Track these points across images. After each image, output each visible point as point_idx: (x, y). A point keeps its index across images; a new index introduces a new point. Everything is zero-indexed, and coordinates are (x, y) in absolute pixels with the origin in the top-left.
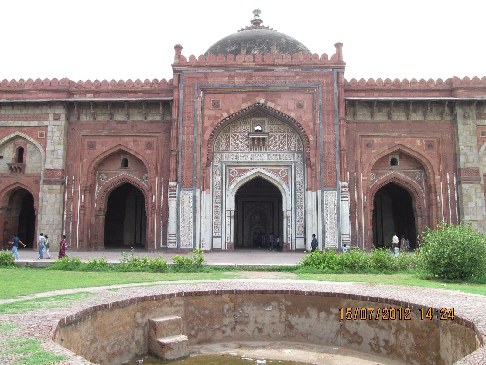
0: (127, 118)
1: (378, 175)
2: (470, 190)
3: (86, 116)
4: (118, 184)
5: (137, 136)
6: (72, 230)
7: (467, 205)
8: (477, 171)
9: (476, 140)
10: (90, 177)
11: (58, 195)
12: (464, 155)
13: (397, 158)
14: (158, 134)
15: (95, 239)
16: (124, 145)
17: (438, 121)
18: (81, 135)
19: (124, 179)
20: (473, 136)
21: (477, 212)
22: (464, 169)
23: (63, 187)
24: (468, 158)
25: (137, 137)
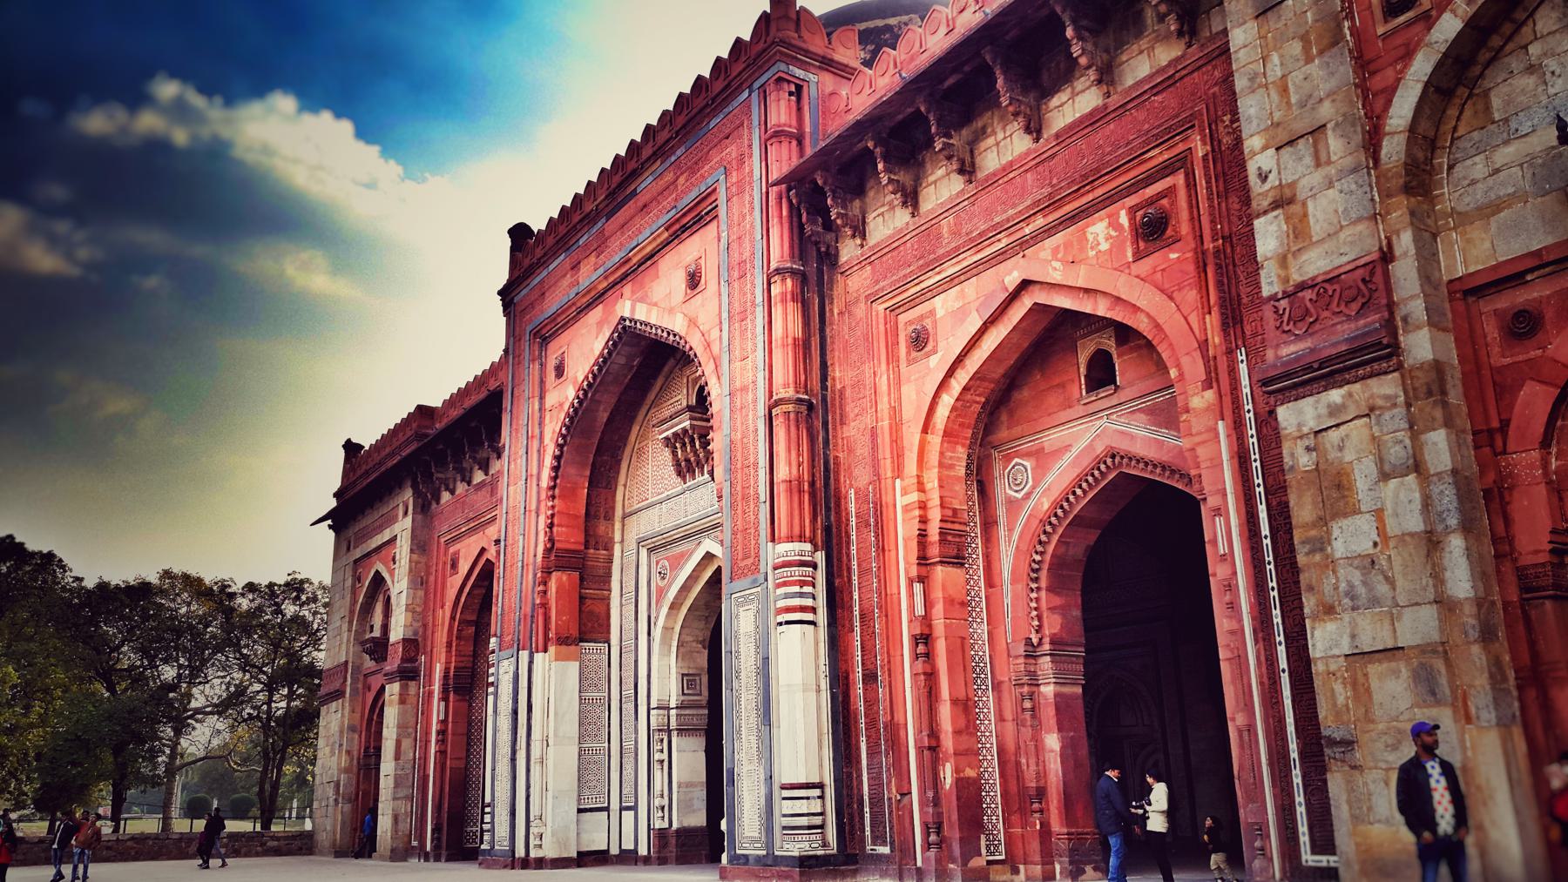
1: (1042, 458)
2: (1334, 436)
7: (1321, 545)
8: (1367, 284)
9: (1345, 70)
12: (1277, 204)
13: (1110, 345)
17: (1169, 65)
20: (1321, 52)
21: (1391, 582)
22: (1284, 303)
24: (1305, 215)
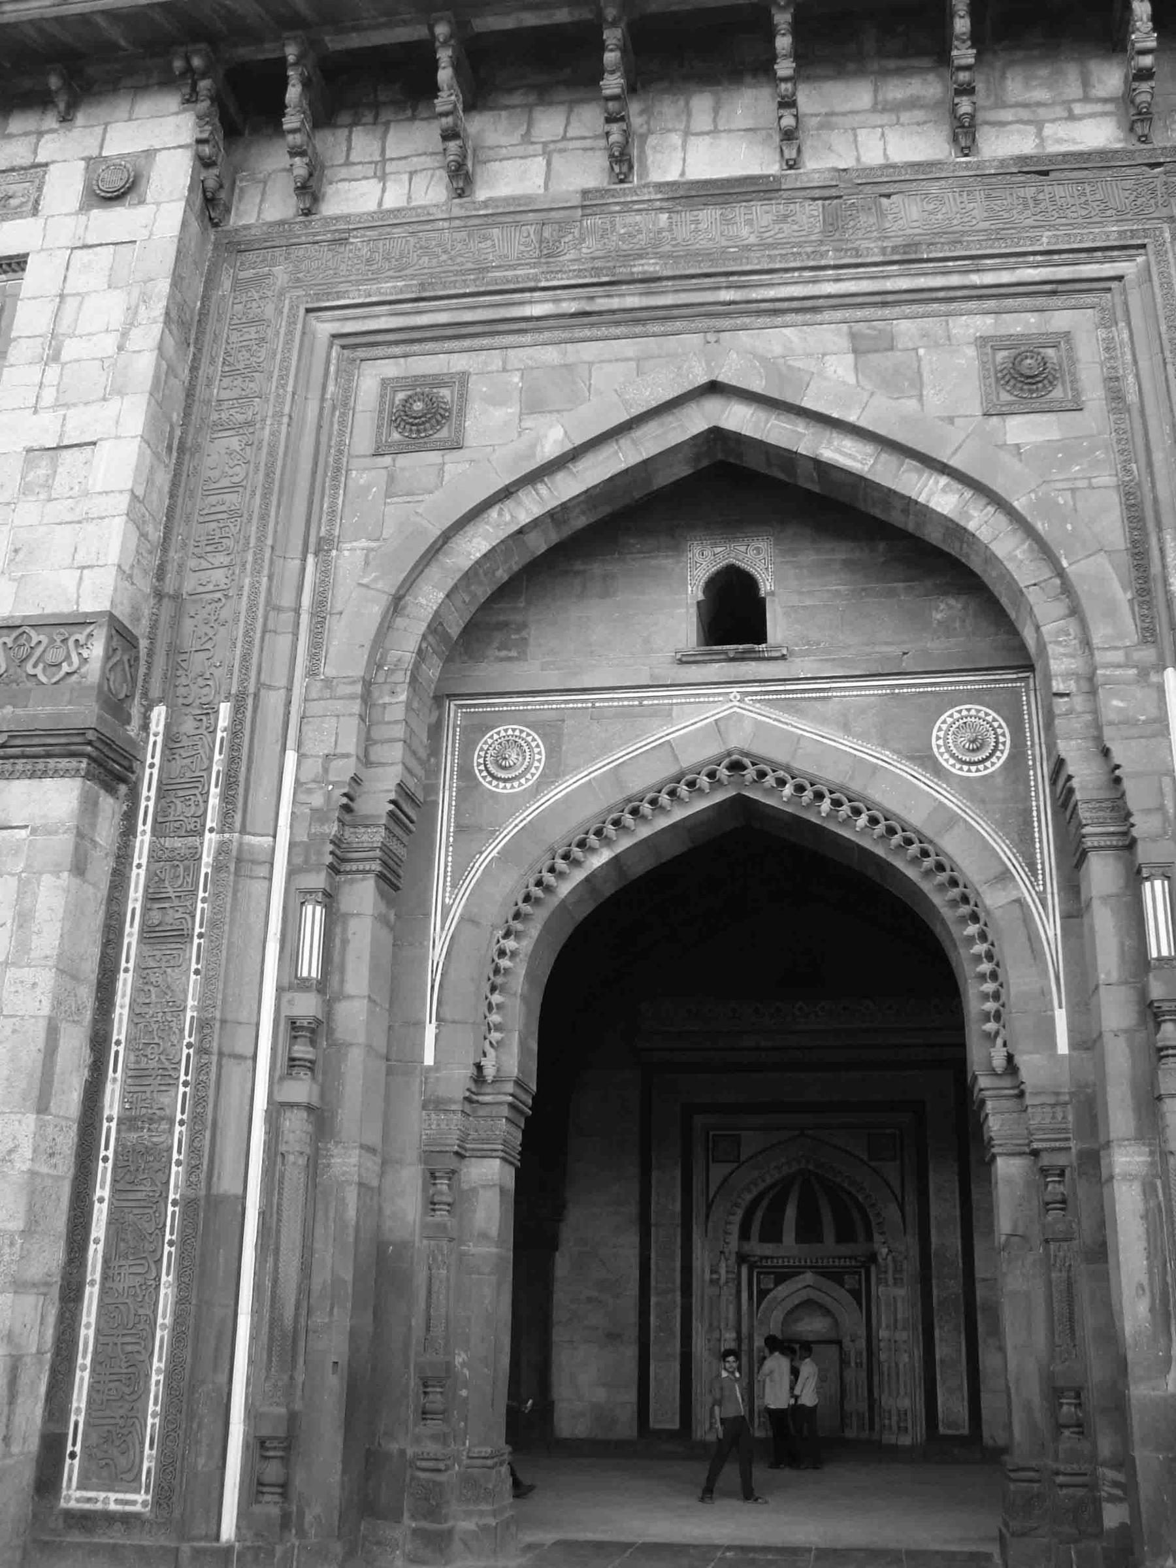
0: (789, 135)
3: (383, 178)
4: (663, 822)
5: (884, 300)
6: (181, 1301)
10: (398, 713)
11: (47, 880)
14: (1108, 270)
15: (425, 1414)
16: (757, 385)
18: (324, 328)
19: (723, 773)
23: (110, 807)
25: (887, 312)
